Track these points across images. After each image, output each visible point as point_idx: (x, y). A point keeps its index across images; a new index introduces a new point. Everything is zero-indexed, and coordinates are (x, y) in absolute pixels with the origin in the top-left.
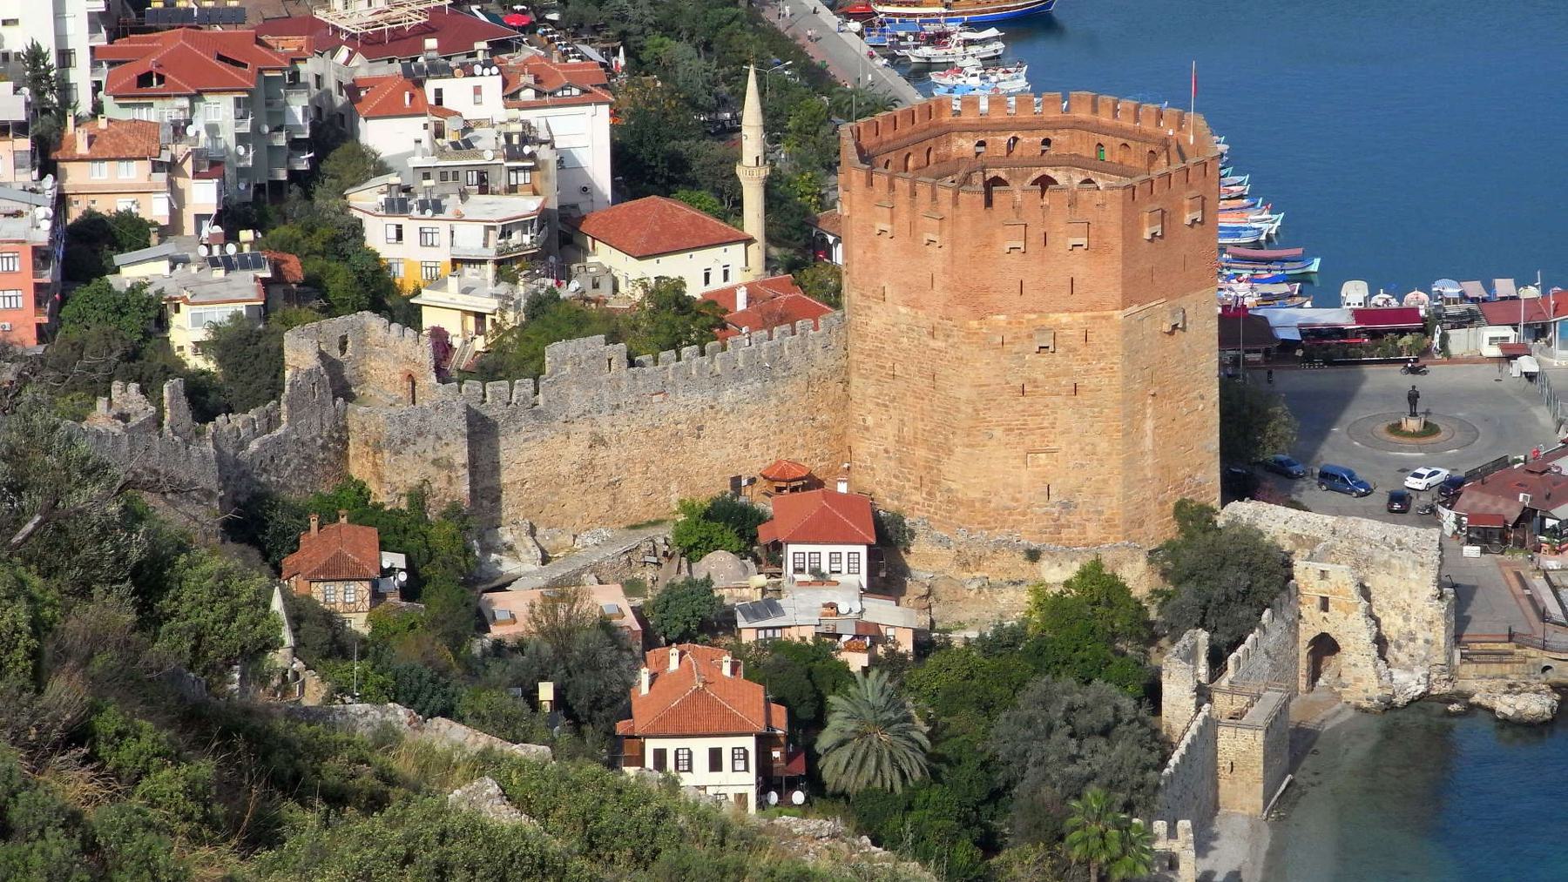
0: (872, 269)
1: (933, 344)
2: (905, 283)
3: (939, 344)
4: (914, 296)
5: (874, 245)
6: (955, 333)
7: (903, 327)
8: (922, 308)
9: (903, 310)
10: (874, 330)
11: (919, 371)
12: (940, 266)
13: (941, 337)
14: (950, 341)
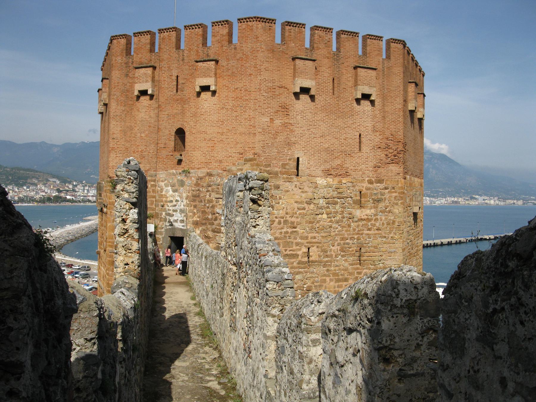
0: (281, 138)
1: (358, 213)
2: (327, 150)
3: (369, 212)
4: (338, 162)
5: (285, 109)
6: (387, 196)
7: (322, 202)
8: (347, 174)
9: (321, 181)
10: (282, 213)
11: (342, 250)
12: (370, 125)
13: (370, 204)
14: (381, 205)
